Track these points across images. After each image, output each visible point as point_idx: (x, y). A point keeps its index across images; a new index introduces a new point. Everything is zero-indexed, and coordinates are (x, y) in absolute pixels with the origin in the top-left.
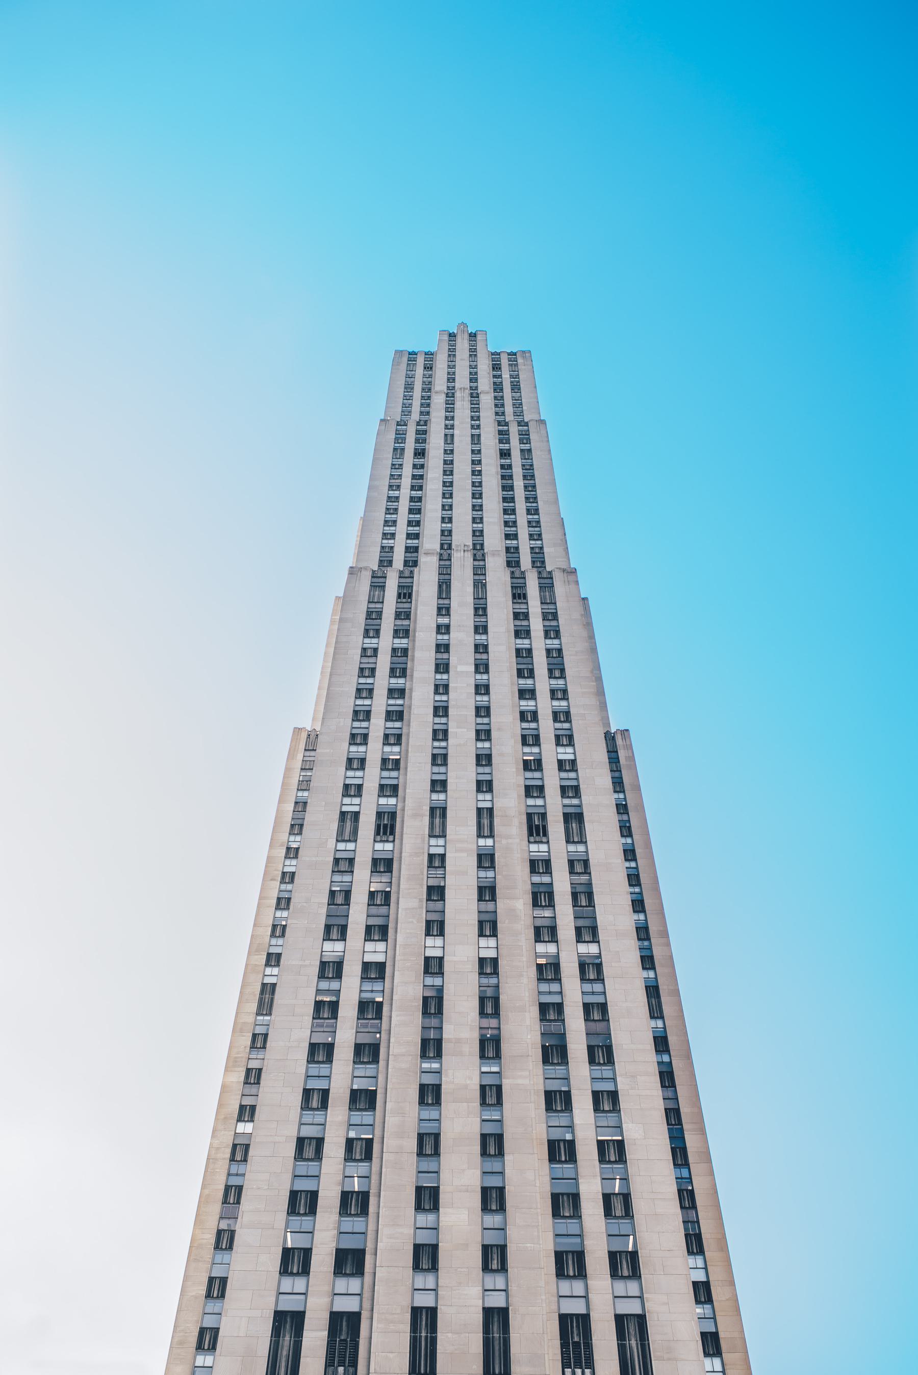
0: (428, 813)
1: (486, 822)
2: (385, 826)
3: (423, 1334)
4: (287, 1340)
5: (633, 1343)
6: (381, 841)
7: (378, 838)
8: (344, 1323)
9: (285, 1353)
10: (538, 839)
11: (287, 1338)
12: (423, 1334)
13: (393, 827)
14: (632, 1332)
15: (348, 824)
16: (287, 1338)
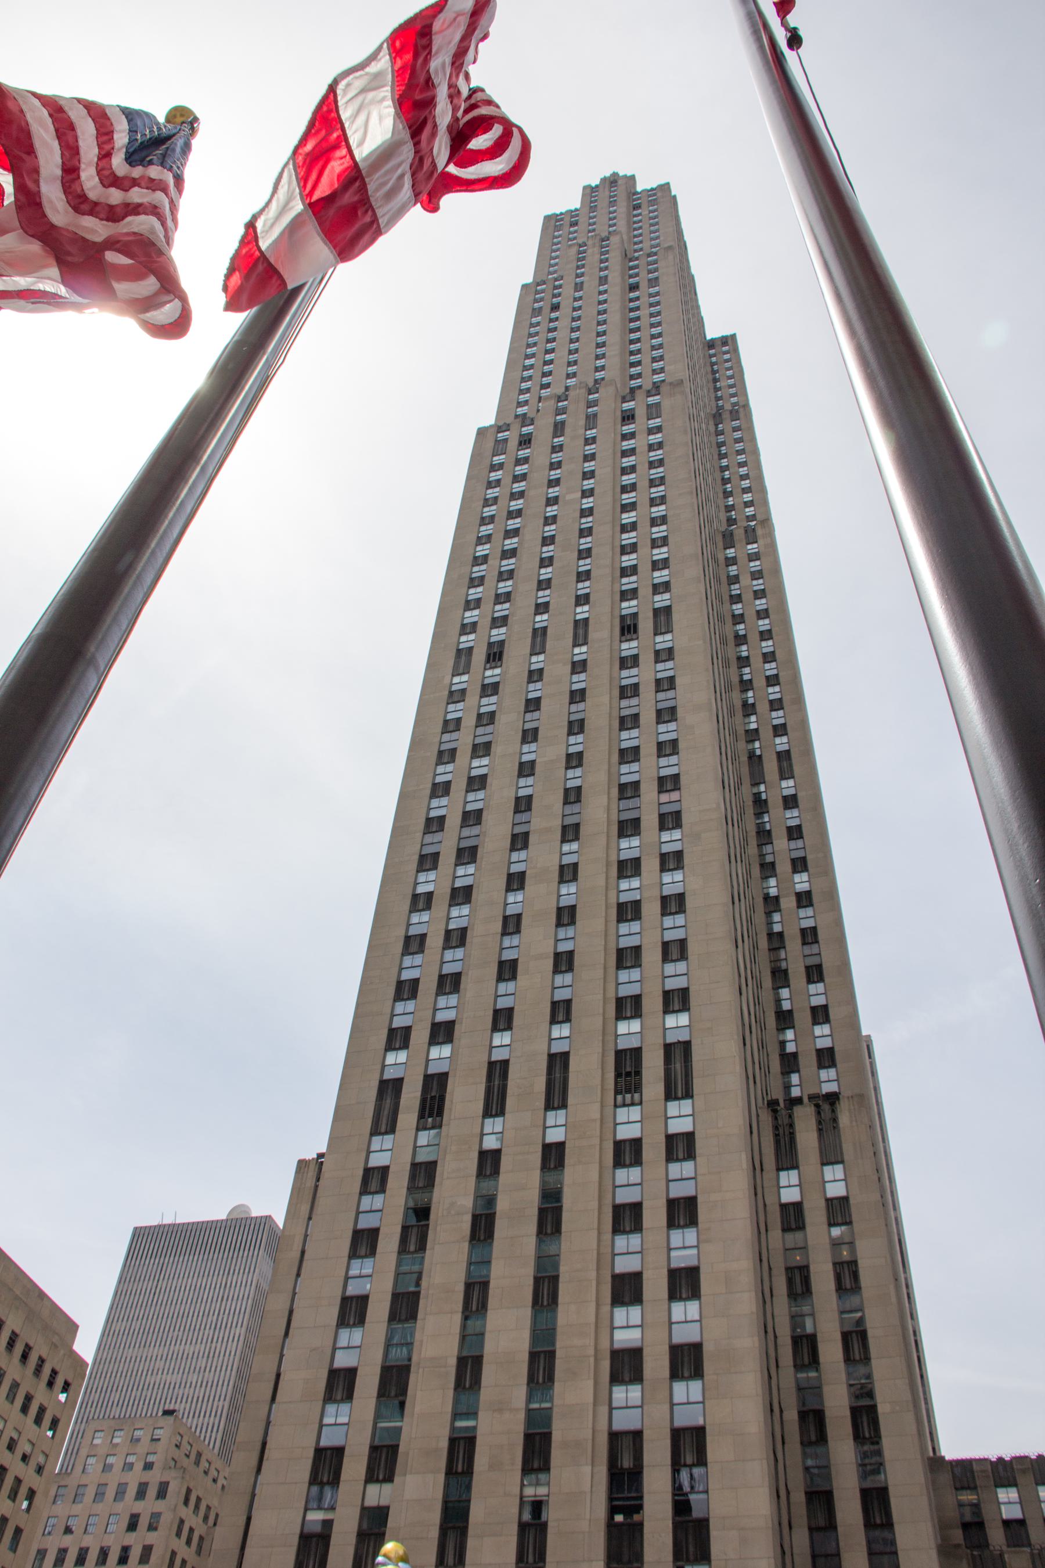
0: (530, 635)
1: (581, 632)
2: (495, 654)
3: (496, 1083)
4: (388, 1103)
5: (678, 1066)
6: (491, 668)
7: (488, 666)
8: (435, 1083)
9: (386, 1112)
10: (629, 637)
11: (388, 1101)
12: (496, 1083)
13: (501, 654)
14: (678, 1057)
15: (463, 658)
16: (388, 1101)
